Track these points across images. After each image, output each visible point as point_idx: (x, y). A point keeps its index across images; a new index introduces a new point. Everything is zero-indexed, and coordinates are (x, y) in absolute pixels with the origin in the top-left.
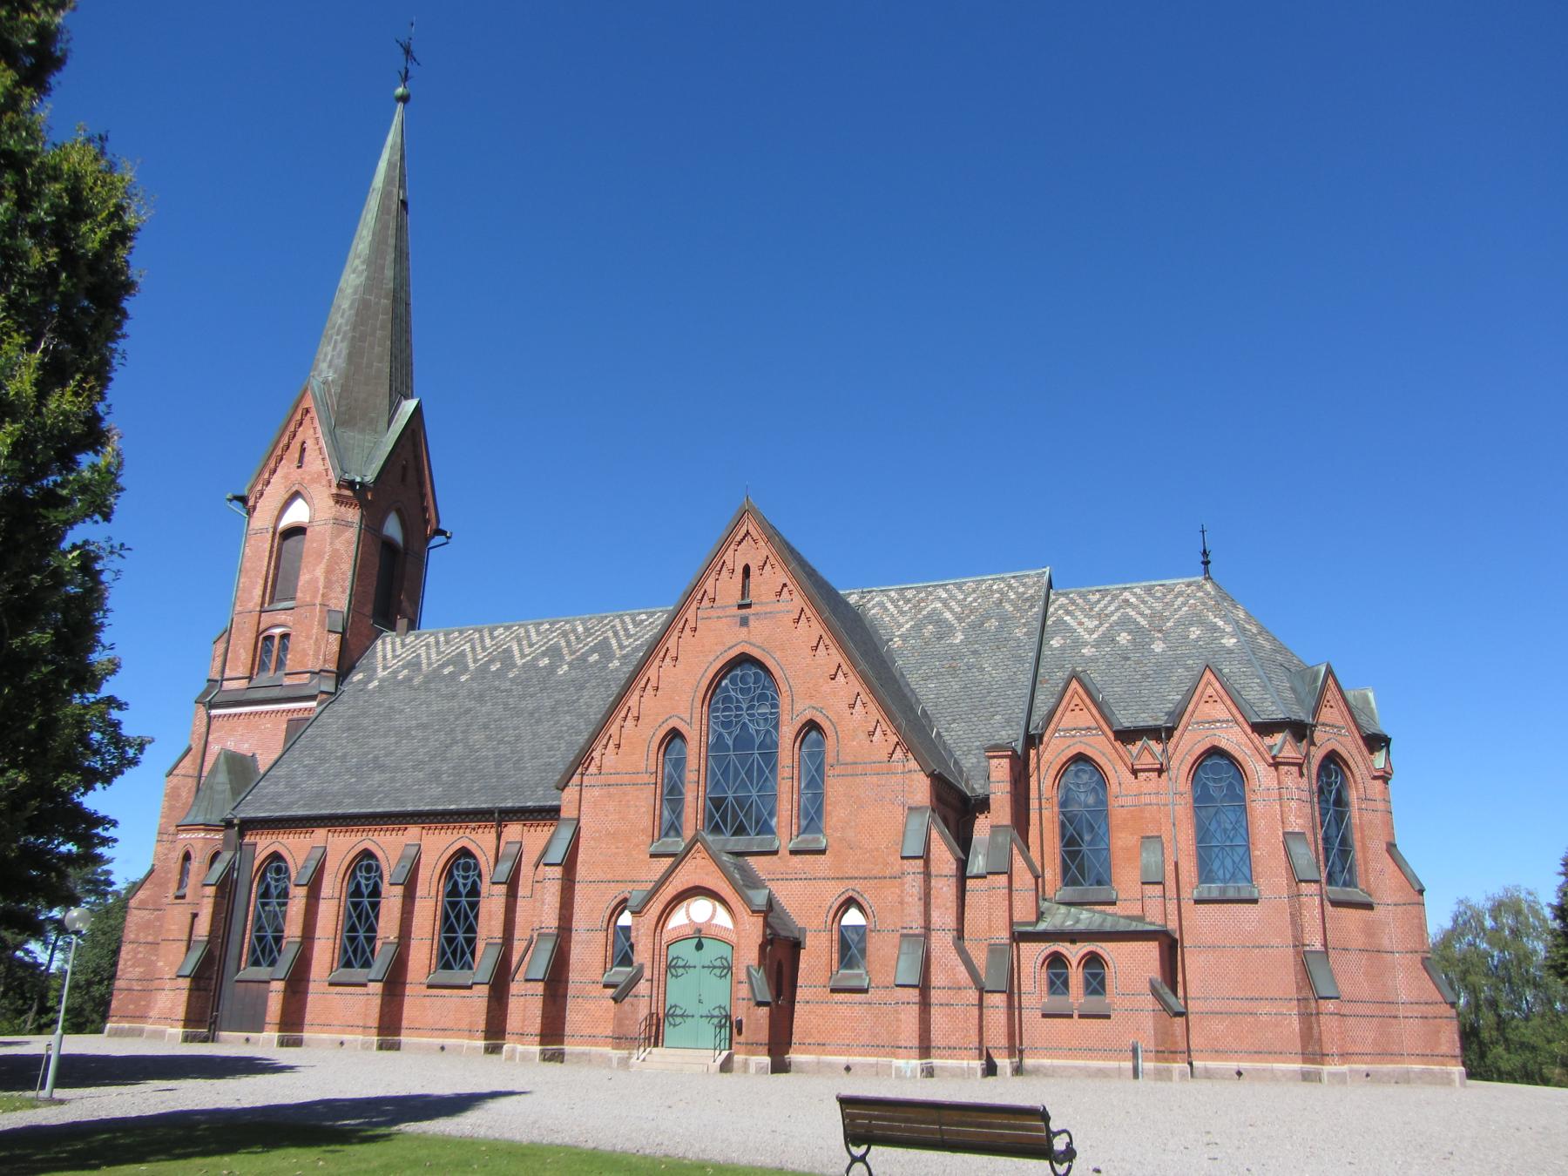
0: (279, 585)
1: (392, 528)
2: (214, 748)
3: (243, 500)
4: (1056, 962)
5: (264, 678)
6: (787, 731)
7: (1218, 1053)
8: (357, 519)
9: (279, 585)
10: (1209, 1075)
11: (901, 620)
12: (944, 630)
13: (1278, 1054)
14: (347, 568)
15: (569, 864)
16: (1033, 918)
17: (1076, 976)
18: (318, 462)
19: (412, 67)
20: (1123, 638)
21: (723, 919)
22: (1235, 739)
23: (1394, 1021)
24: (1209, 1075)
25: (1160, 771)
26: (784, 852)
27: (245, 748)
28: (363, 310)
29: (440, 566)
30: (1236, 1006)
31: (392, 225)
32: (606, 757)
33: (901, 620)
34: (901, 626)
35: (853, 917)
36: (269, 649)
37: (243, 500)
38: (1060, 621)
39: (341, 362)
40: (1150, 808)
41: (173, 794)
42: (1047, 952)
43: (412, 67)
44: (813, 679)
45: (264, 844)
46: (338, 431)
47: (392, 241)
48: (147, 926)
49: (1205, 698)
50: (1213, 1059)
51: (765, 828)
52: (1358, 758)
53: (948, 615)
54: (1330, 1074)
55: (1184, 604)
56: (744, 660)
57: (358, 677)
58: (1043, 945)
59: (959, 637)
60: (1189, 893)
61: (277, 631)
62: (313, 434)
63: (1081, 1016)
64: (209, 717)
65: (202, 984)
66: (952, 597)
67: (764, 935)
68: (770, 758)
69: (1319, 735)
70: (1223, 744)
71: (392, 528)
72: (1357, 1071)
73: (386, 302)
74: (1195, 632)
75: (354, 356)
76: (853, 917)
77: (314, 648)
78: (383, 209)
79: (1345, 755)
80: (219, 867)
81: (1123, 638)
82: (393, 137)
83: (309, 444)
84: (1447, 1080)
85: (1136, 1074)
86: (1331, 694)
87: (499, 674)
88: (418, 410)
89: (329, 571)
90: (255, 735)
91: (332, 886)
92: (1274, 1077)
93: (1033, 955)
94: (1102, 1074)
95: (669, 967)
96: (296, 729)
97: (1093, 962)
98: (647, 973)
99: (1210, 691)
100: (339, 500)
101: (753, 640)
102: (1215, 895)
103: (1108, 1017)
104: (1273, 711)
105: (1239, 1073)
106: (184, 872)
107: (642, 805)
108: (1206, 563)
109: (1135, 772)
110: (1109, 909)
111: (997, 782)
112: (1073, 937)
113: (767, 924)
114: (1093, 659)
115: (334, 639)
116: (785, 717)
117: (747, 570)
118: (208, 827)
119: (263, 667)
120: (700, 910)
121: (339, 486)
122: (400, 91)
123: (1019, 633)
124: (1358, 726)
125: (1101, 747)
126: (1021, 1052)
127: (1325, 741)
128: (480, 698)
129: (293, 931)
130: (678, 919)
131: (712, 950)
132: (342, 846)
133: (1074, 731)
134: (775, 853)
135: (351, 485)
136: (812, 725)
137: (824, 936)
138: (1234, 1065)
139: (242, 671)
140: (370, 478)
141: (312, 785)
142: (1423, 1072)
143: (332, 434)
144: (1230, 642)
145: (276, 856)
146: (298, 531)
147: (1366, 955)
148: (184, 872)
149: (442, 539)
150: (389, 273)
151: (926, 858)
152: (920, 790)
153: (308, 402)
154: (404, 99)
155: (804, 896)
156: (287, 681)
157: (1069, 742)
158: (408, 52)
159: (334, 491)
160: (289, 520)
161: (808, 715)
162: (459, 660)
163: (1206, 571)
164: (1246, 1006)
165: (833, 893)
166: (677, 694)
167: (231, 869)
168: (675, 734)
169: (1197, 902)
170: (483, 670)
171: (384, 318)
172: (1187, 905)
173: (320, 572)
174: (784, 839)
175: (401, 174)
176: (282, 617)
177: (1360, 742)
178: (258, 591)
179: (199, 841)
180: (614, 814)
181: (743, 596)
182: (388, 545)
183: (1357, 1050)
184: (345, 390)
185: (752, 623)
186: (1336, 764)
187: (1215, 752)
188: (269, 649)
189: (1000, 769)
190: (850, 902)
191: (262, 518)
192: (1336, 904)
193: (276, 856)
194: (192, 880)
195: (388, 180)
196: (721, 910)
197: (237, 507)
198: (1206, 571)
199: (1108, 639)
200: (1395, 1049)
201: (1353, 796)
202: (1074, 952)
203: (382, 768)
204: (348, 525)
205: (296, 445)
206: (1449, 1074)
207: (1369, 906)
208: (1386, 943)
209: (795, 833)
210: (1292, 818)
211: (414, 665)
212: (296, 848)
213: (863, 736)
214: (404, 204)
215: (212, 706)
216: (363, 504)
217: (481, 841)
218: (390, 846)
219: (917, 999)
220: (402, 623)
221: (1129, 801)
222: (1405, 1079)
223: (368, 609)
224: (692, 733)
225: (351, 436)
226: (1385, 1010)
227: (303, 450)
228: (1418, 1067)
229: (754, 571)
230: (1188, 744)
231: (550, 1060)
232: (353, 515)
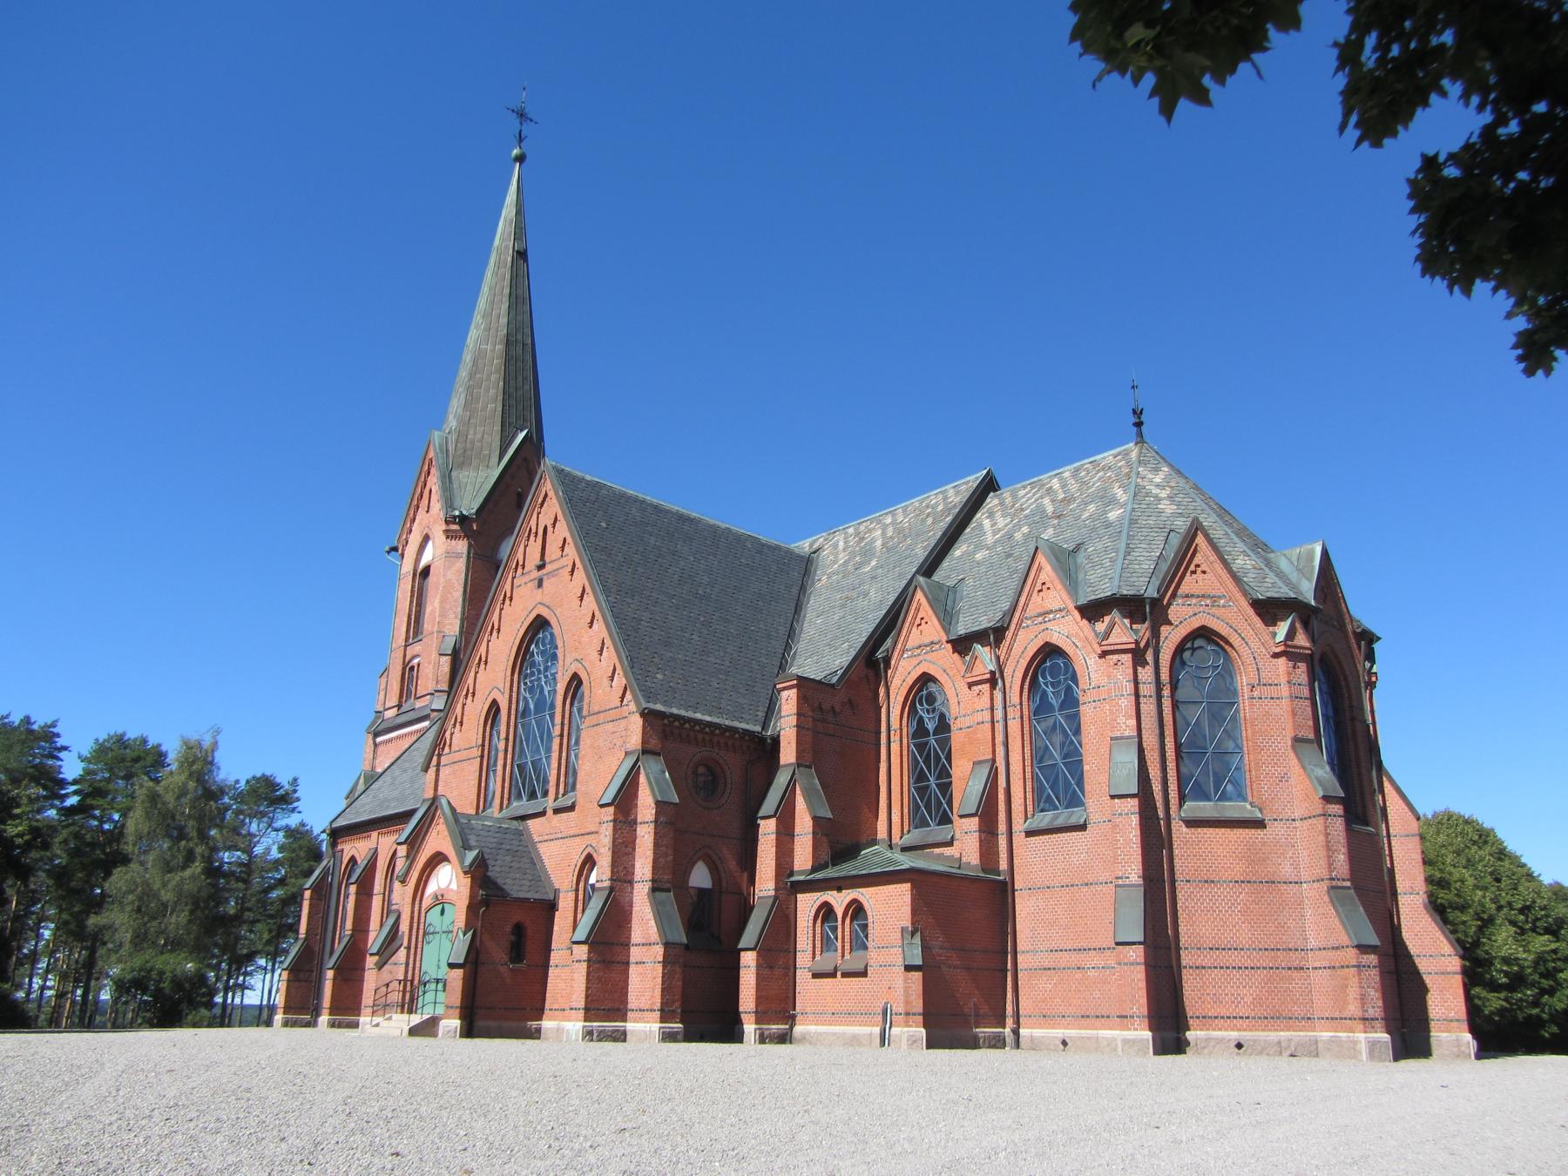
3: (395, 549)
4: (826, 912)
7: (1046, 1018)
8: (465, 550)
10: (1035, 1046)
13: (1102, 1018)
16: (809, 866)
17: (845, 929)
19: (527, 129)
22: (1069, 632)
23: (1295, 974)
24: (1035, 1046)
25: (992, 681)
26: (549, 812)
30: (1065, 959)
31: (508, 277)
37: (395, 549)
38: (980, 525)
42: (818, 903)
43: (527, 129)
46: (454, 474)
47: (507, 291)
49: (1038, 587)
50: (1040, 1026)
51: (1075, 801)
52: (1248, 633)
54: (1126, 1041)
58: (816, 895)
60: (1019, 826)
62: (434, 482)
63: (845, 975)
64: (376, 745)
65: (301, 975)
67: (472, 896)
69: (1176, 611)
70: (1056, 639)
72: (1220, 1041)
73: (500, 347)
78: (498, 265)
79: (1223, 630)
84: (1351, 1052)
85: (883, 1039)
86: (1204, 556)
89: (443, 601)
92: (1096, 1046)
93: (807, 904)
94: (854, 1041)
95: (425, 934)
99: (1043, 577)
100: (449, 535)
102: (1044, 825)
103: (864, 974)
104: (1105, 590)
105: (1064, 1043)
108: (1139, 425)
109: (970, 685)
110: (947, 851)
112: (839, 885)
116: (559, 676)
119: (408, 697)
121: (447, 522)
122: (516, 152)
124: (1245, 593)
126: (793, 1017)
127: (1183, 617)
133: (921, 650)
134: (543, 814)
137: (572, 895)
138: (1060, 1033)
139: (395, 701)
142: (1331, 1041)
147: (1247, 887)
150: (504, 320)
151: (624, 801)
153: (431, 454)
154: (521, 159)
156: (419, 704)
157: (915, 661)
158: (522, 115)
159: (444, 527)
160: (423, 563)
163: (1140, 434)
164: (1075, 959)
168: (495, 705)
169: (1030, 833)
172: (1019, 838)
173: (437, 604)
175: (520, 231)
177: (1251, 612)
178: (404, 629)
183: (1224, 1012)
184: (461, 435)
185: (545, 583)
186: (1218, 644)
187: (1050, 652)
192: (1192, 823)
193: (353, 860)
197: (393, 558)
198: (1140, 434)
200: (1297, 1010)
201: (1243, 681)
202: (839, 900)
204: (458, 556)
206: (1355, 1042)
207: (1259, 824)
208: (1286, 871)
209: (561, 790)
210: (1121, 720)
213: (606, 682)
215: (376, 735)
219: (585, 957)
221: (967, 721)
222: (1313, 1050)
226: (1284, 960)
228: (1326, 1035)
229: (550, 529)
230: (1022, 646)
231: (340, 1026)
232: (462, 546)
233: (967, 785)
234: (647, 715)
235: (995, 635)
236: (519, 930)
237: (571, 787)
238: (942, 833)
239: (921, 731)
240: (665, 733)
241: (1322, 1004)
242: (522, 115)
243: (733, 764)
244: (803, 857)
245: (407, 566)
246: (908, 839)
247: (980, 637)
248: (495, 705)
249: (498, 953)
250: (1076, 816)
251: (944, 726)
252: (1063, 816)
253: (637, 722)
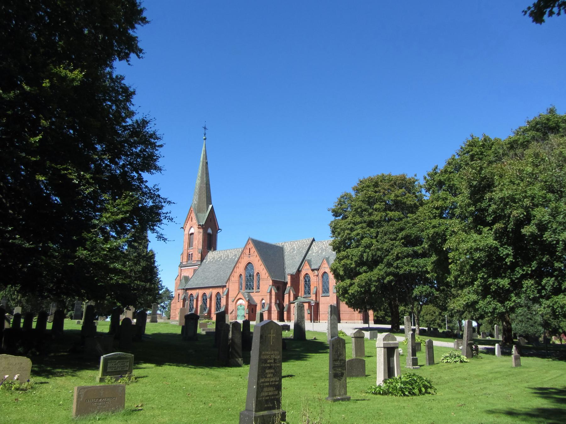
0: (190, 244)
1: (210, 231)
2: (182, 275)
5: (189, 262)
6: (255, 274)
9: (190, 244)
14: (201, 241)
15: (227, 295)
18: (195, 221)
27: (187, 275)
28: (200, 188)
29: (220, 237)
32: (232, 279)
35: (264, 301)
36: (189, 256)
39: (197, 200)
40: (315, 281)
41: (176, 283)
43: (207, 131)
44: (259, 267)
45: (190, 292)
48: (175, 306)
56: (249, 263)
57: (205, 261)
60: (320, 296)
68: (253, 278)
71: (210, 231)
73: (205, 185)
75: (199, 198)
76: (264, 301)
77: (197, 256)
78: (203, 165)
80: (183, 297)
82: (203, 149)
87: (226, 260)
88: (212, 207)
89: (198, 242)
90: (188, 272)
91: (200, 299)
93: (292, 305)
96: (195, 271)
100: (199, 228)
101: (251, 260)
106: (179, 297)
107: (236, 286)
111: (288, 279)
113: (249, 302)
115: (200, 254)
118: (182, 289)
120: (240, 302)
125: (310, 272)
128: (223, 265)
129: (195, 306)
131: (243, 307)
132: (201, 292)
133: (306, 270)
135: (200, 225)
136: (258, 273)
140: (204, 223)
141: (196, 282)
143: (196, 215)
145: (191, 294)
146: (192, 234)
148: (179, 297)
149: (219, 231)
150: (205, 179)
151: (271, 292)
153: (192, 209)
154: (205, 139)
155: (256, 298)
158: (205, 128)
160: (190, 233)
162: (220, 257)
166: (241, 269)
167: (185, 297)
168: (241, 275)
170: (224, 259)
171: (205, 189)
173: (196, 242)
174: (254, 291)
175: (206, 157)
176: (191, 250)
179: (181, 292)
180: (233, 287)
182: (209, 234)
187: (325, 272)
188: (189, 256)
190: (263, 299)
191: (186, 232)
193: (191, 294)
194: (180, 298)
195: (203, 159)
203: (206, 278)
211: (214, 258)
212: (194, 293)
214: (207, 163)
216: (203, 228)
217: (220, 290)
218: (208, 292)
220: (212, 249)
223: (206, 248)
224: (243, 275)
225: (200, 215)
232: (201, 230)
233: (313, 290)
234: (273, 281)
235: (318, 270)
236: (252, 309)
237: (259, 288)
238: (309, 295)
239: (306, 281)
240: (275, 283)
241: (356, 318)
242: (205, 128)
243: (281, 286)
244: (292, 299)
245: (186, 232)
246: (305, 296)
247: (316, 269)
248: (241, 275)
249: (251, 312)
250: (328, 294)
251: (309, 281)
252: (326, 294)
253: (271, 281)
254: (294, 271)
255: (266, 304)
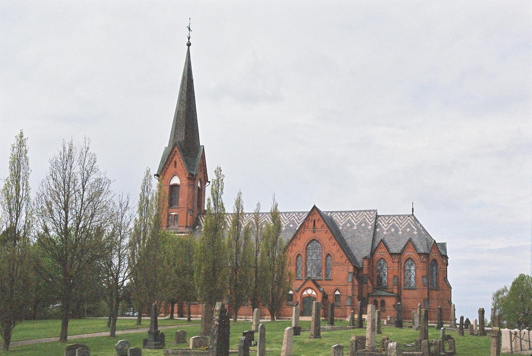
11: (342, 221)
12: (352, 226)
20: (393, 230)
21: (314, 293)
33: (342, 221)
34: (342, 223)
43: (191, 33)
53: (353, 221)
55: (407, 221)
59: (355, 228)
61: (174, 214)
66: (354, 216)
74: (408, 230)
76: (337, 293)
81: (393, 230)
83: (178, 161)
97: (383, 302)
98: (300, 303)
104: (422, 251)
112: (379, 296)
114: (386, 235)
117: (314, 220)
120: (309, 291)
123: (370, 227)
130: (305, 293)
144: (415, 233)
146: (176, 186)
152: (351, 269)
161: (328, 252)
165: (333, 288)
181: (314, 226)
189: (366, 262)
196: (314, 292)
199: (389, 230)
205: (174, 159)
227: (175, 162)
254: (366, 253)
255: (343, 299)
